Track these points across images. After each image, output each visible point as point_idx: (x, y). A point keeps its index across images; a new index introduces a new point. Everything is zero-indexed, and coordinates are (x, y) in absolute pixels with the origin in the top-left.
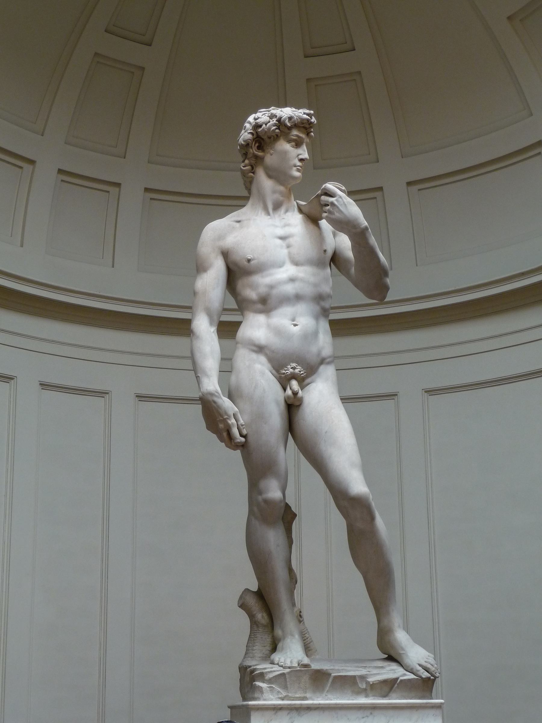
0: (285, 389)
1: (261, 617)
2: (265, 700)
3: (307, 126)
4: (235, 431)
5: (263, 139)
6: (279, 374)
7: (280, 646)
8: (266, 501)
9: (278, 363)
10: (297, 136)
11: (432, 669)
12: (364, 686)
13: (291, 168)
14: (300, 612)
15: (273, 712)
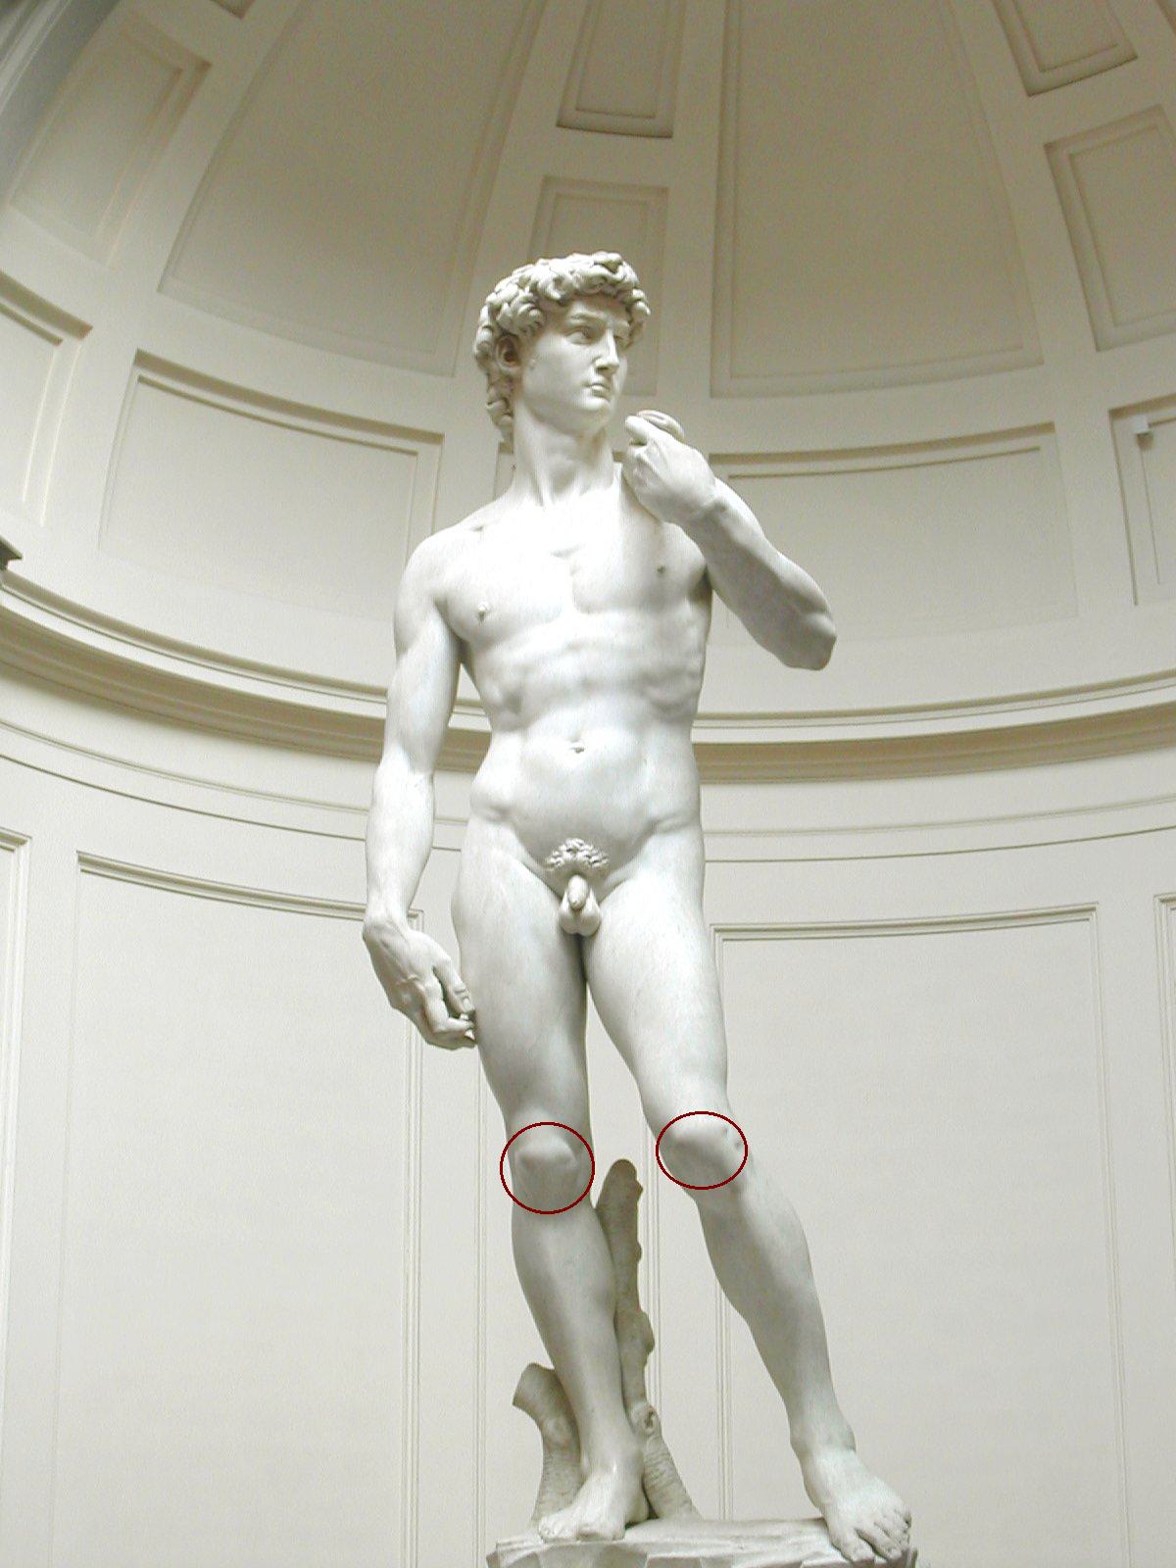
0: (560, 898)
1: (555, 1424)
3: (610, 290)
4: (437, 1008)
5: (515, 336)
10: (582, 317)
13: (577, 391)
14: (651, 1413)
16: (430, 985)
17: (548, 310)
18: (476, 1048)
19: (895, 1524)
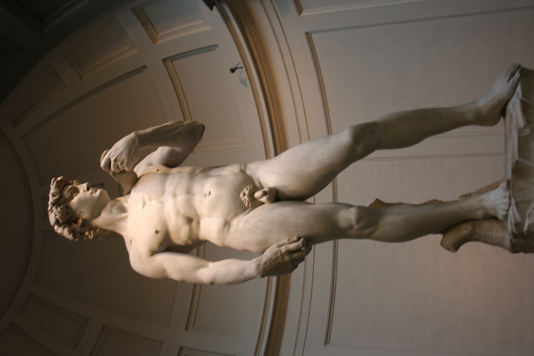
0: (263, 203)
1: (465, 230)
3: (64, 183)
4: (292, 246)
5: (69, 219)
6: (248, 207)
7: (491, 212)
8: (358, 221)
9: (241, 208)
11: (512, 70)
13: (92, 198)
14: (462, 196)
16: (283, 249)
17: (62, 202)
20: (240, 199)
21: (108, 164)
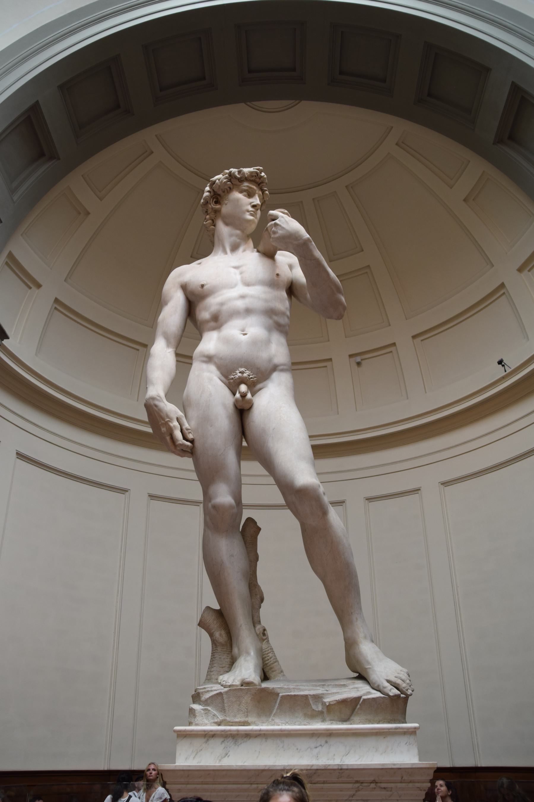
0: (234, 394)
2: (197, 725)
4: (178, 434)
6: (228, 380)
8: (215, 507)
12: (320, 708)
15: (204, 740)
18: (191, 459)
19: (404, 676)
20: (237, 369)
21: (273, 218)
